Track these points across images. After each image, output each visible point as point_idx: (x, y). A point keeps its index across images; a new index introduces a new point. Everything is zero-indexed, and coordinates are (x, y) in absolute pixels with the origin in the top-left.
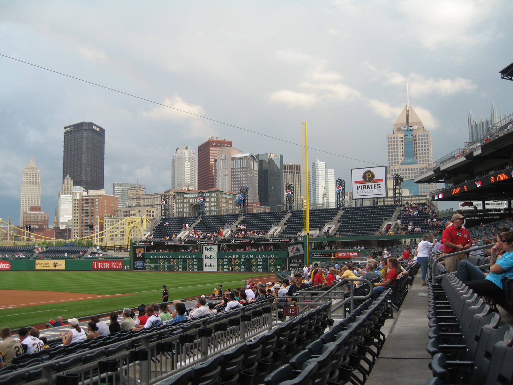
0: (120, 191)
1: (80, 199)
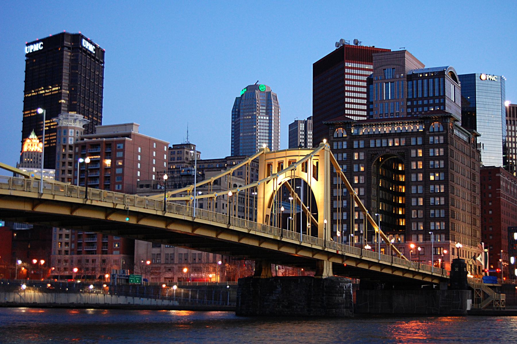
1: (76, 145)
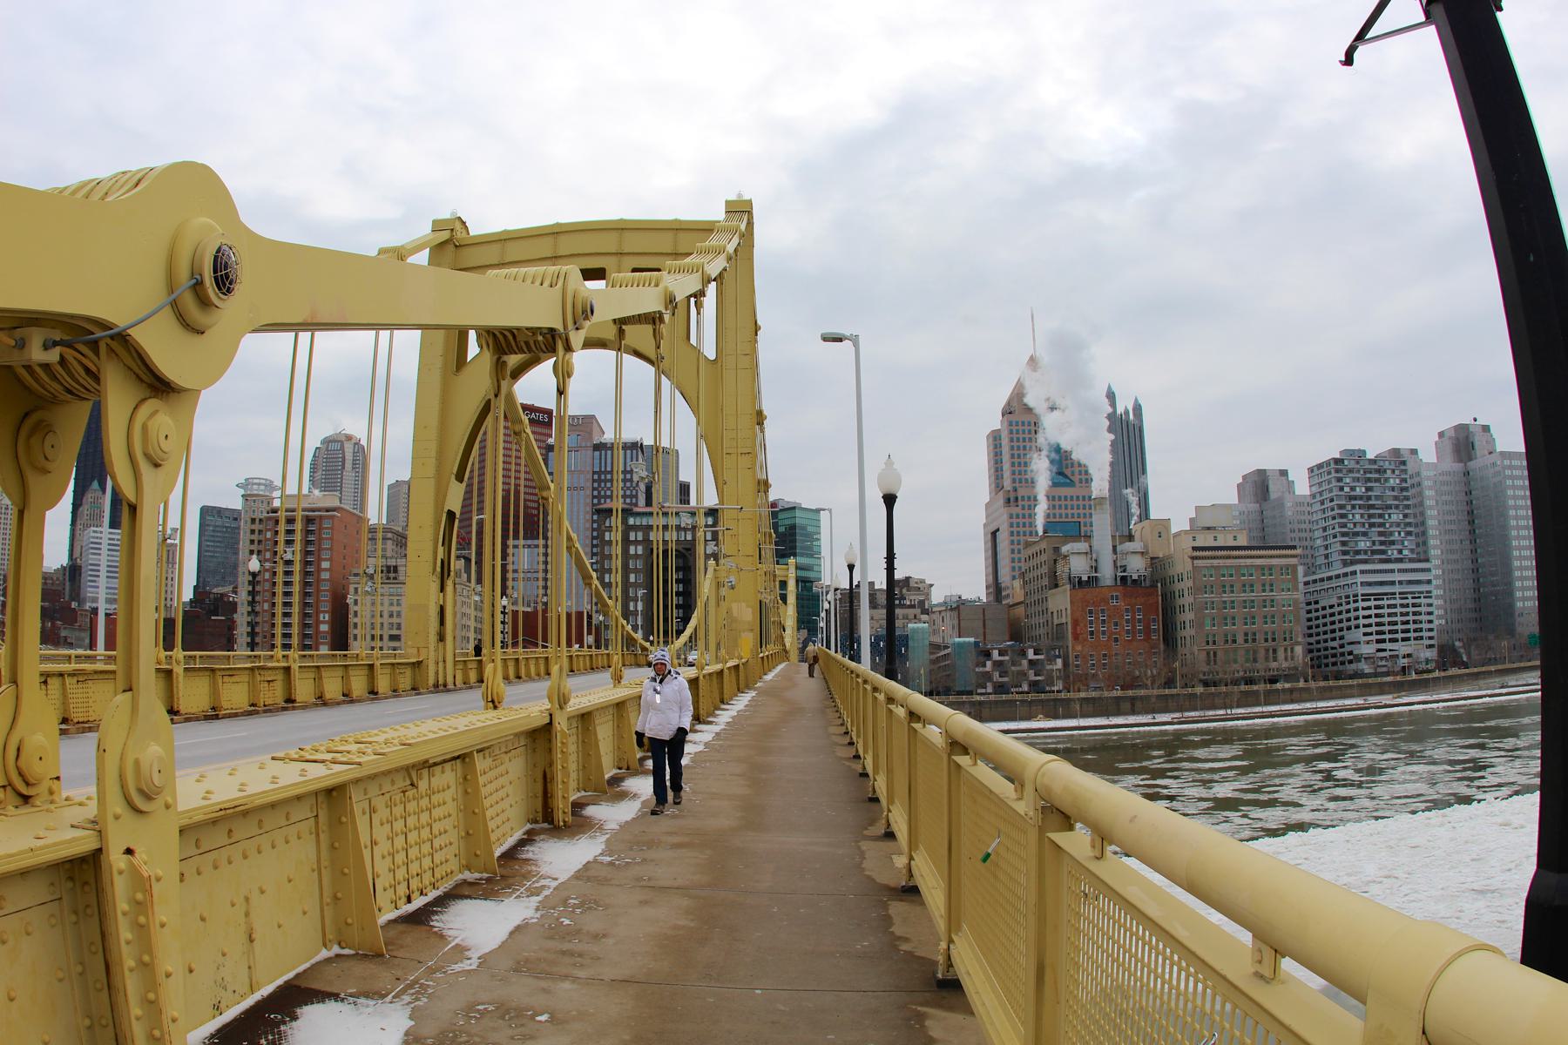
0: (218, 526)
